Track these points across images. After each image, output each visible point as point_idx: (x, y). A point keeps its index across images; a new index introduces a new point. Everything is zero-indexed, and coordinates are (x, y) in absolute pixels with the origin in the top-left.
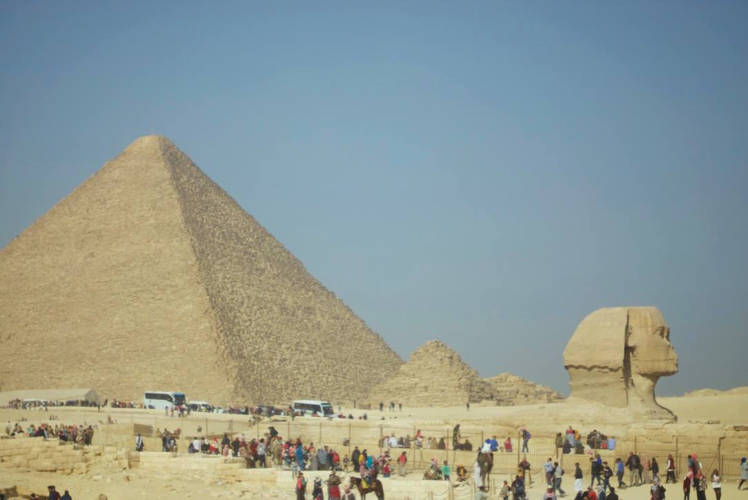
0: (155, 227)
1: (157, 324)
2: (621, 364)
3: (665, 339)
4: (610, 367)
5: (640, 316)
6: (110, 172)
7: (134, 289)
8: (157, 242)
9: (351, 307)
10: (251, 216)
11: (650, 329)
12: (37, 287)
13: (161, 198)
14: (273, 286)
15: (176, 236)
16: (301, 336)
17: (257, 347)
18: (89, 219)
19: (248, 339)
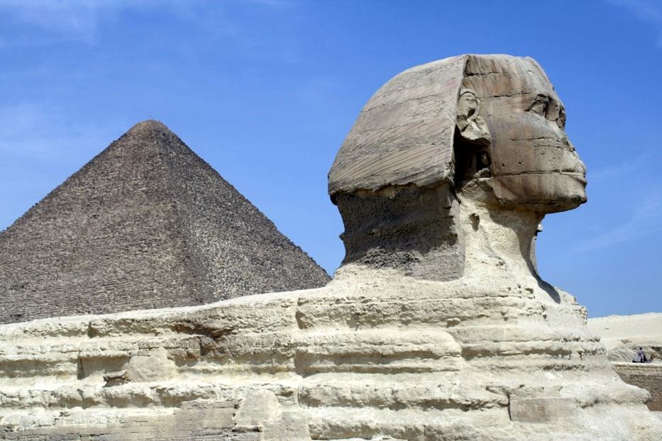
0: (146, 193)
1: (142, 272)
2: (446, 173)
3: (554, 127)
4: (419, 184)
5: (495, 72)
6: (114, 150)
7: (125, 244)
8: (147, 204)
9: (314, 259)
10: (232, 186)
11: (518, 99)
12: (49, 244)
13: (152, 170)
14: (246, 241)
15: (163, 199)
16: (267, 281)
17: (226, 290)
18: (94, 188)
19: (219, 283)
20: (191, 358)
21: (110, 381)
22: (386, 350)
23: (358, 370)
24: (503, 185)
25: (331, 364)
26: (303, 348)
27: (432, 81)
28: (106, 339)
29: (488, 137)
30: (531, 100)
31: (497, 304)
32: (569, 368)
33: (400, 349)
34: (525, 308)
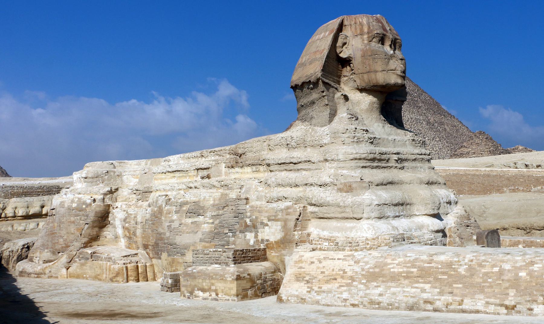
11: (366, 36)
20: (232, 167)
21: (202, 178)
22: (294, 161)
23: (286, 170)
24: (360, 79)
25: (277, 167)
26: (267, 162)
27: (326, 31)
28: (207, 159)
29: (352, 56)
30: (372, 36)
31: (340, 137)
32: (385, 168)
33: (299, 160)
34: (356, 138)
